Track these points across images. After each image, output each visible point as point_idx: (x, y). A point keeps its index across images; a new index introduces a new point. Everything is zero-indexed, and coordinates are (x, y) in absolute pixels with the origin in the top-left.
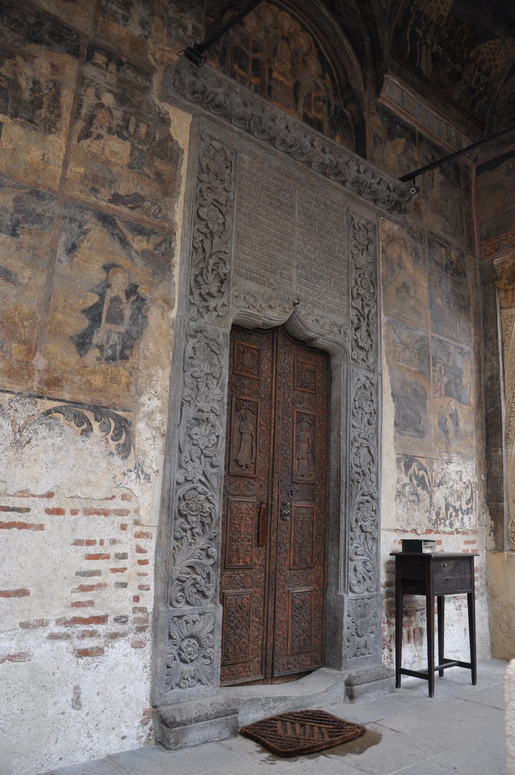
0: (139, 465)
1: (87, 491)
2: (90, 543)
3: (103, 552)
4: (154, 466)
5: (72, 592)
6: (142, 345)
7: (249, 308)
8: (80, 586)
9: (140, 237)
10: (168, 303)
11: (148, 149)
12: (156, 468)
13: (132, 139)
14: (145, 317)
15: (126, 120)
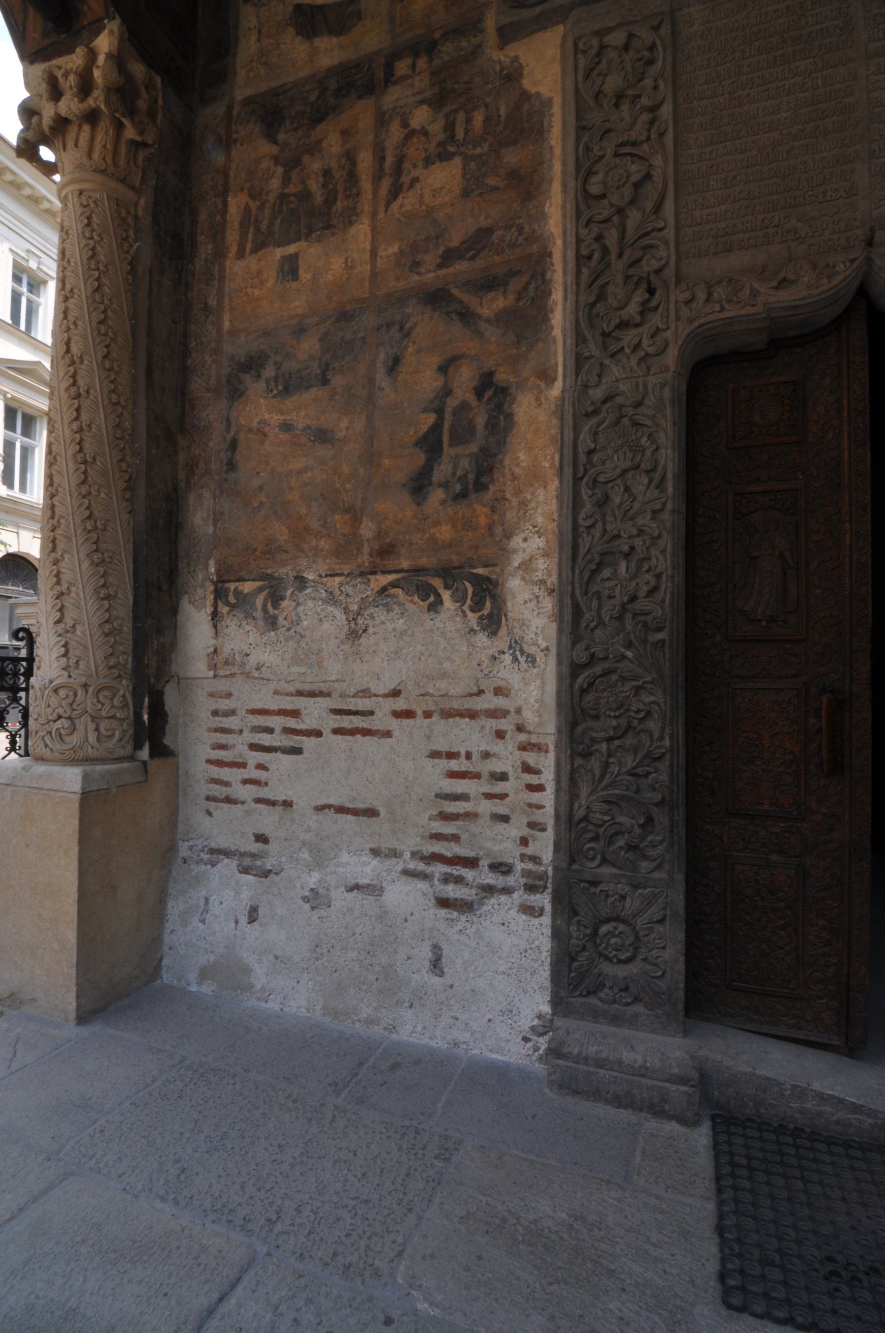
0: (516, 642)
1: (442, 685)
2: (451, 755)
3: (471, 769)
4: (540, 640)
5: (430, 819)
6: (507, 462)
7: (722, 309)
8: (441, 813)
9: (492, 294)
10: (546, 376)
11: (490, 146)
12: (544, 645)
13: (462, 150)
14: (510, 416)
15: (450, 127)
